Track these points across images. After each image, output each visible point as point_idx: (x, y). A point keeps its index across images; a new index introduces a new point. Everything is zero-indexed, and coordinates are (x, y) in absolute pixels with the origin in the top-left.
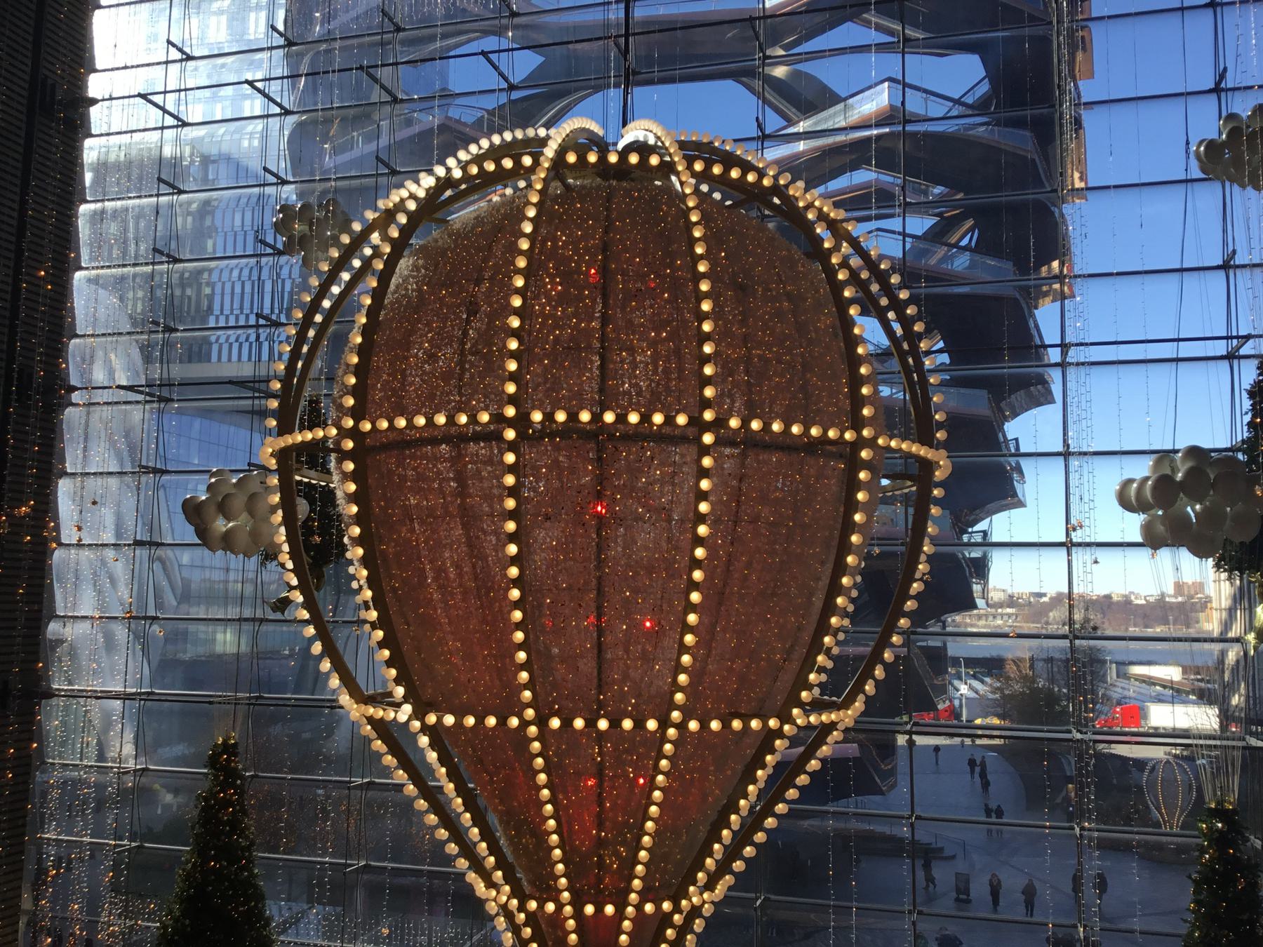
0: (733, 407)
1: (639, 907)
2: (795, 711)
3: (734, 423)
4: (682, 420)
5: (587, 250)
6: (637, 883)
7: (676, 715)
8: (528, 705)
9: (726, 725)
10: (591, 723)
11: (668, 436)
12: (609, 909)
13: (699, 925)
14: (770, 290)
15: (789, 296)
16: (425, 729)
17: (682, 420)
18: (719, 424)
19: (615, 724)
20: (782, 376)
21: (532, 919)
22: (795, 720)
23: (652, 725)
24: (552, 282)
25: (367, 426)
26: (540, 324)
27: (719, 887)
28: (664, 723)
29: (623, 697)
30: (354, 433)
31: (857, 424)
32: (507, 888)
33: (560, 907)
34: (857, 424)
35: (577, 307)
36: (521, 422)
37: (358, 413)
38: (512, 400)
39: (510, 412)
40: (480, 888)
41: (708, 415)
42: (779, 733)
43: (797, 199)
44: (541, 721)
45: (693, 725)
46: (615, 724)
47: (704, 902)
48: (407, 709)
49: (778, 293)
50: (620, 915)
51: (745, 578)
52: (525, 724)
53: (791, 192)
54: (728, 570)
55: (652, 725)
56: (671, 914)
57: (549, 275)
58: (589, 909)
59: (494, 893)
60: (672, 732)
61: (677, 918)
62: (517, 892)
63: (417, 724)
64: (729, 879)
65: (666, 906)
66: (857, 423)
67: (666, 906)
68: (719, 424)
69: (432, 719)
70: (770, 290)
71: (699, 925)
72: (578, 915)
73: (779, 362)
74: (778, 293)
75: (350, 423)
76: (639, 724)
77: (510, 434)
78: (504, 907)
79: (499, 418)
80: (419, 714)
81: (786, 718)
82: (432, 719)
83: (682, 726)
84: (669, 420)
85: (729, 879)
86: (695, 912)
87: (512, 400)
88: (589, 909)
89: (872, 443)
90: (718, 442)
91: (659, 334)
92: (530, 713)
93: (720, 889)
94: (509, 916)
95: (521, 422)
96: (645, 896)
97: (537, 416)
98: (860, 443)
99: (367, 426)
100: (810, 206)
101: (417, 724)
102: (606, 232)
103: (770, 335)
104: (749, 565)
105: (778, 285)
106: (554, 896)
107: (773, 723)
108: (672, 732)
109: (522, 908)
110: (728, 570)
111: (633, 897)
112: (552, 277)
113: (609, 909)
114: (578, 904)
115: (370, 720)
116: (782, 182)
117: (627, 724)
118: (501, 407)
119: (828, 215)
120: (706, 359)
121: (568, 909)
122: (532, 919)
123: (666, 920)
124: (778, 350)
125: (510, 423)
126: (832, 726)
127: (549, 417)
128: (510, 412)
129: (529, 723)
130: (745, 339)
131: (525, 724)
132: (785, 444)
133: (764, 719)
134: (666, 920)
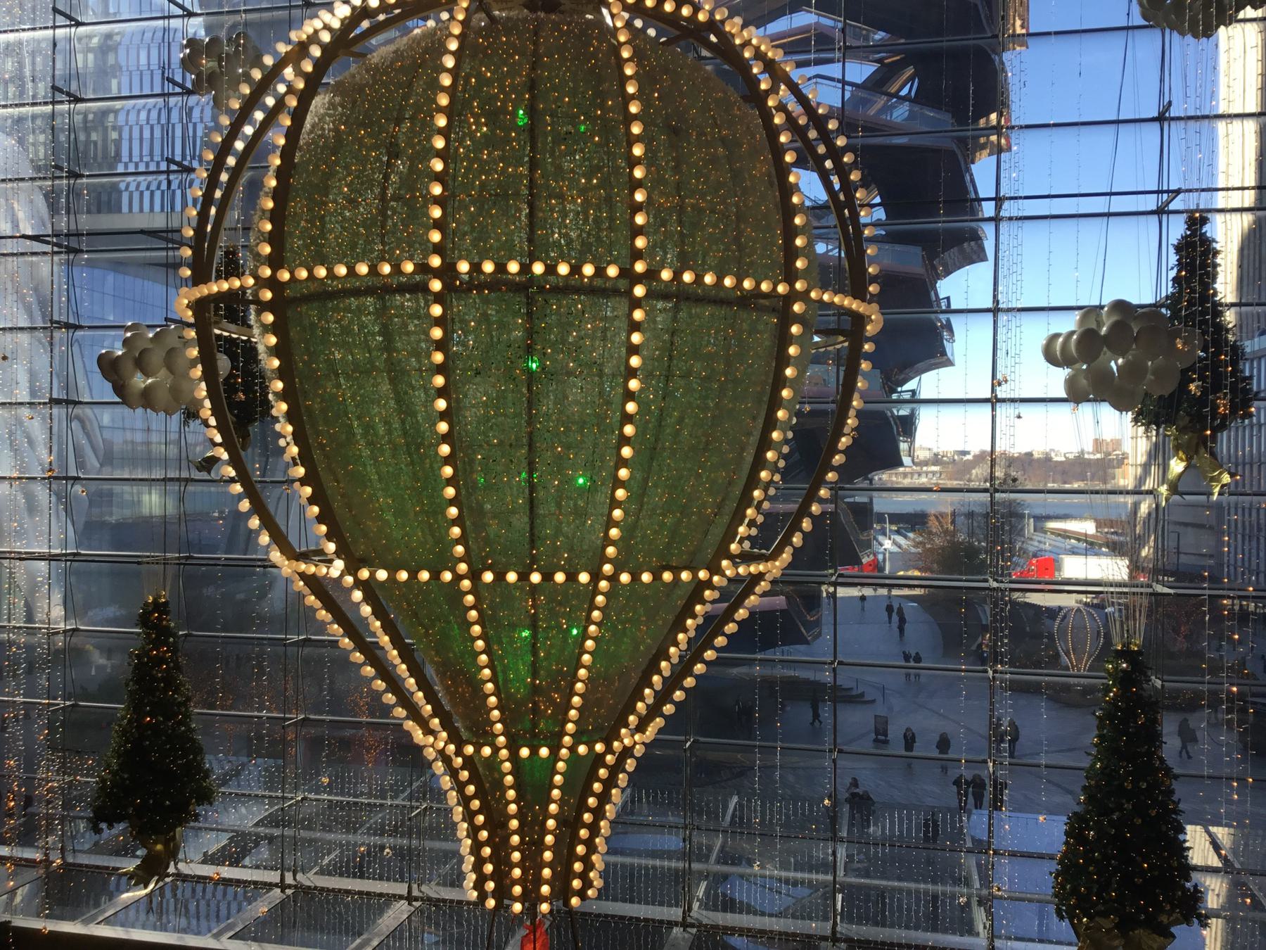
0: (666, 258)
1: (572, 749)
2: (725, 563)
3: (666, 275)
4: (612, 271)
5: (514, 89)
6: (570, 727)
7: (607, 568)
8: (461, 560)
9: (657, 577)
10: (524, 577)
11: (599, 290)
12: (544, 752)
13: (630, 765)
14: (705, 135)
15: (724, 141)
16: (358, 584)
17: (612, 271)
18: (651, 276)
19: (548, 577)
20: (715, 226)
21: (469, 763)
22: (724, 571)
23: (584, 578)
24: (477, 123)
25: (285, 276)
26: (465, 168)
27: (650, 729)
28: (596, 576)
29: (556, 552)
30: (272, 283)
32: (444, 734)
33: (496, 750)
37: (276, 262)
38: (438, 249)
39: (436, 261)
40: (418, 735)
41: (640, 267)
42: (709, 584)
43: (733, 36)
44: (475, 575)
45: (625, 578)
46: (548, 577)
47: (635, 743)
48: (339, 565)
51: (677, 433)
52: (458, 578)
53: (727, 29)
54: (660, 426)
55: (584, 578)
56: (603, 755)
57: (473, 115)
58: (525, 752)
59: (431, 739)
60: (603, 584)
61: (610, 759)
62: (454, 737)
63: (349, 580)
64: (659, 722)
65: (599, 747)
66: (790, 276)
67: (599, 747)
68: (651, 276)
69: (364, 574)
70: (705, 135)
71: (630, 765)
72: (514, 757)
75: (267, 272)
76: (572, 577)
77: (436, 285)
78: (442, 753)
79: (423, 268)
80: (351, 569)
81: (715, 569)
82: (364, 574)
83: (613, 579)
84: (600, 272)
85: (659, 722)
86: (627, 752)
87: (438, 249)
88: (525, 752)
89: (804, 296)
90: (649, 295)
91: (589, 180)
92: (463, 567)
93: (651, 732)
94: (447, 760)
95: (447, 273)
96: (578, 738)
97: (464, 267)
98: (792, 296)
99: (285, 276)
100: (747, 43)
101: (349, 580)
102: (533, 69)
103: (704, 183)
104: (681, 421)
105: (713, 129)
106: (490, 739)
107: (703, 575)
108: (603, 584)
109: (459, 752)
110: (660, 426)
112: (477, 117)
113: (544, 752)
114: (513, 748)
115: (303, 576)
116: (718, 17)
117: (560, 577)
118: (426, 257)
119: (766, 54)
120: (637, 208)
121: (504, 753)
122: (469, 763)
123: (599, 760)
124: (712, 199)
125: (437, 273)
126: (760, 576)
127: (476, 268)
128: (436, 261)
129: (462, 577)
130: (679, 187)
131: (458, 578)
132: (717, 297)
133: (694, 570)
134: (599, 760)
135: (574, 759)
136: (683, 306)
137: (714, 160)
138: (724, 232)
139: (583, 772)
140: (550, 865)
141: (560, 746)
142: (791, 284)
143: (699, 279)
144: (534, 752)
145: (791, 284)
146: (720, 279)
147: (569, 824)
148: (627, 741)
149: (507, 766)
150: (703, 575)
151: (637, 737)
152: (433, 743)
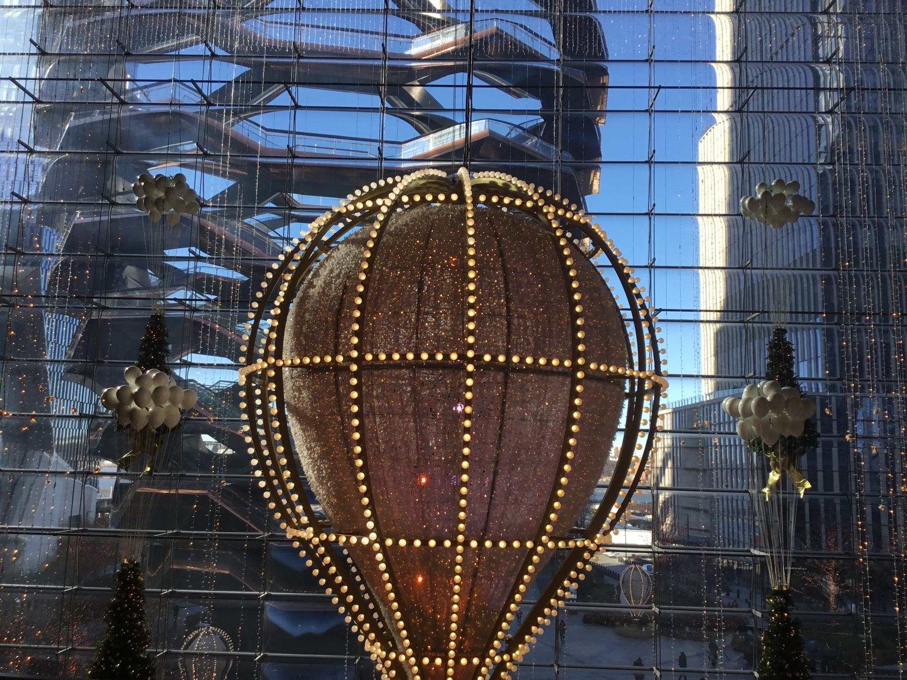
1: (457, 660)
3: (487, 358)
12: (438, 661)
17: (454, 356)
18: (478, 357)
23: (448, 543)
28: (455, 543)
31: (575, 355)
36: (360, 360)
38: (356, 347)
41: (470, 354)
42: (533, 551)
44: (381, 540)
55: (448, 543)
58: (426, 661)
65: (476, 661)
67: (476, 661)
68: (478, 357)
72: (419, 663)
76: (440, 543)
77: (354, 368)
82: (324, 537)
87: (356, 347)
88: (426, 661)
92: (373, 536)
93: (516, 654)
95: (360, 360)
108: (460, 548)
113: (438, 661)
114: (419, 657)
121: (413, 660)
128: (355, 354)
131: (371, 544)
142: (574, 361)
144: (432, 661)
145: (574, 361)
151: (505, 657)
152: (376, 651)
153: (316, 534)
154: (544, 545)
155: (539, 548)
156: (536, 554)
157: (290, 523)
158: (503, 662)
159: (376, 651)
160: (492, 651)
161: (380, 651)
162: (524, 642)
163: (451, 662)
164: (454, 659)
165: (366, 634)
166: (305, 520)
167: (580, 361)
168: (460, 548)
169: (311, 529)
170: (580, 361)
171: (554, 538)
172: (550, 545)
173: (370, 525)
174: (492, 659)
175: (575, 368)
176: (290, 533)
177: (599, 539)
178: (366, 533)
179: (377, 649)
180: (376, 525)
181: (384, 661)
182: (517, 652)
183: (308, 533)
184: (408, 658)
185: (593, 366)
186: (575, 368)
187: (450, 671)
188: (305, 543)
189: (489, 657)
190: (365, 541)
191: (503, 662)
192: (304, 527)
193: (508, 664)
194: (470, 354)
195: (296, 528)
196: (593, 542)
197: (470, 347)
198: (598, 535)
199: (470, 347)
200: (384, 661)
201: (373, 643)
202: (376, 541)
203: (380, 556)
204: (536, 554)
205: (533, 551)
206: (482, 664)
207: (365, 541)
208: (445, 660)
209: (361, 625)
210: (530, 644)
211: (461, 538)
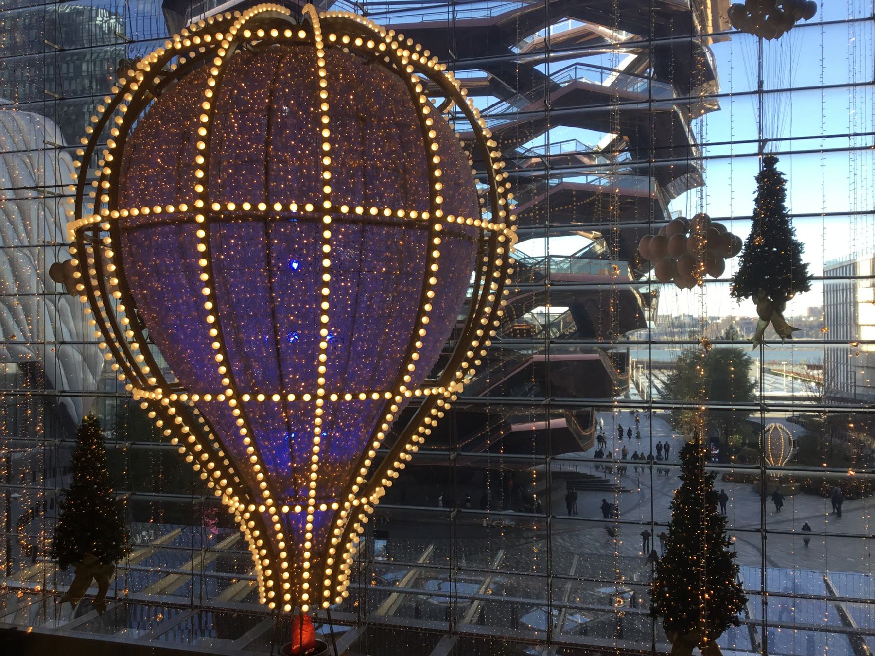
1: (316, 506)
6: (312, 493)
11: (302, 218)
14: (383, 121)
15: (397, 125)
20: (389, 177)
28: (315, 397)
30: (110, 219)
33: (268, 508)
34: (432, 208)
35: (250, 135)
38: (201, 196)
41: (327, 205)
42: (392, 401)
44: (238, 396)
49: (389, 123)
50: (304, 513)
54: (357, 302)
55: (307, 397)
57: (234, 113)
65: (335, 506)
67: (335, 506)
72: (279, 512)
73: (387, 168)
74: (389, 123)
77: (200, 218)
81: (396, 392)
82: (174, 397)
87: (201, 196)
92: (230, 392)
93: (374, 498)
96: (319, 499)
102: (273, 83)
104: (370, 299)
107: (388, 395)
108: (320, 402)
110: (357, 302)
111: (312, 501)
112: (235, 114)
113: (298, 509)
121: (273, 510)
124: (386, 161)
128: (200, 204)
131: (228, 399)
135: (317, 513)
136: (368, 228)
137: (389, 137)
138: (395, 181)
139: (325, 522)
140: (308, 581)
141: (308, 506)
142: (432, 212)
143: (380, 212)
145: (432, 212)
146: (394, 212)
147: (320, 554)
148: (356, 503)
149: (276, 518)
150: (388, 395)
151: (364, 500)
152: (234, 504)
153: (166, 395)
154: (402, 395)
155: (398, 399)
156: (395, 403)
157: (136, 385)
158: (361, 505)
159: (234, 504)
160: (351, 496)
161: (237, 505)
162: (380, 485)
163: (311, 509)
164: (313, 506)
165: (224, 489)
166: (153, 381)
167: (439, 214)
168: (320, 402)
169: (160, 390)
170: (439, 214)
171: (410, 387)
172: (408, 394)
173: (226, 381)
174: (351, 502)
175: (433, 220)
176: (138, 394)
177: (453, 387)
178: (223, 390)
179: (235, 502)
180: (232, 381)
181: (242, 513)
182: (375, 495)
183: (158, 394)
184: (268, 508)
185: (450, 219)
186: (433, 220)
187: (310, 518)
188: (155, 405)
189: (348, 501)
190: (222, 398)
191: (361, 505)
192: (152, 389)
193: (365, 507)
194: (327, 205)
195: (145, 389)
196: (447, 390)
197: (327, 197)
198: (452, 383)
199: (327, 197)
200: (242, 513)
201: (231, 497)
202: (231, 398)
203: (237, 412)
204: (395, 403)
205: (392, 401)
206: (342, 508)
207: (222, 398)
208: (305, 507)
209: (217, 481)
210: (385, 487)
211: (321, 392)
